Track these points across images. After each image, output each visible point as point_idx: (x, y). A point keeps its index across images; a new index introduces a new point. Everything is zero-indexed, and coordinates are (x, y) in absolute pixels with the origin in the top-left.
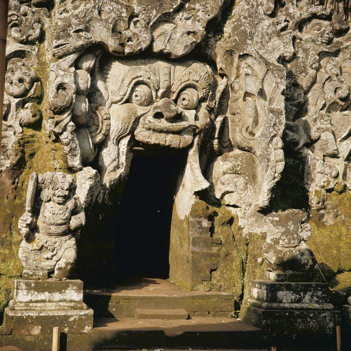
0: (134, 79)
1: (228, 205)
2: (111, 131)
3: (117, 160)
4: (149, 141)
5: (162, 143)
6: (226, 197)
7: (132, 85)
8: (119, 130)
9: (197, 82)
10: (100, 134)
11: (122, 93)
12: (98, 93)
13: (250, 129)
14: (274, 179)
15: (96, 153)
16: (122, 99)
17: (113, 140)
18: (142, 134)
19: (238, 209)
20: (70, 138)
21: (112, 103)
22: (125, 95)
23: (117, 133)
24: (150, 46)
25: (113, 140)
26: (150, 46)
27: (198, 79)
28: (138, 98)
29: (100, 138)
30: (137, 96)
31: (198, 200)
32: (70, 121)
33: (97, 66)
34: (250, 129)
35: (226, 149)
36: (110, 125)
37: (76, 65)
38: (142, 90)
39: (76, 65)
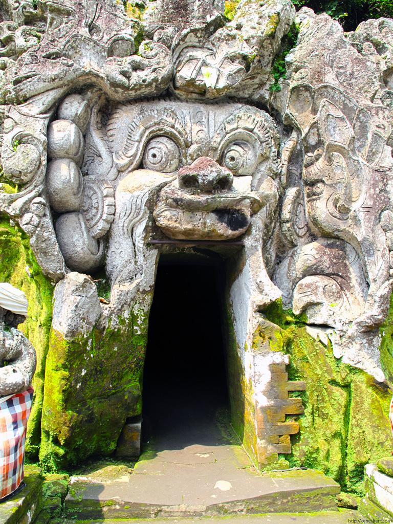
0: (146, 129)
1: (313, 325)
2: (117, 215)
3: (133, 261)
4: (178, 225)
5: (200, 227)
6: (309, 312)
7: (144, 139)
8: (128, 213)
9: (252, 131)
10: (101, 220)
11: (131, 153)
12: (97, 160)
13: (341, 203)
14: (388, 280)
15: (100, 253)
16: (131, 163)
17: (123, 229)
18: (167, 218)
19: (329, 331)
20: (36, 220)
21: (119, 172)
22: (135, 155)
23: (126, 217)
24: (172, 78)
25: (123, 229)
26: (172, 78)
27: (252, 127)
28: (158, 158)
29: (100, 228)
30: (154, 156)
31: (261, 319)
32: (39, 195)
33: (94, 119)
34: (341, 203)
35: (302, 240)
36: (115, 206)
37: (54, 113)
38: (163, 147)
39: (54, 113)
